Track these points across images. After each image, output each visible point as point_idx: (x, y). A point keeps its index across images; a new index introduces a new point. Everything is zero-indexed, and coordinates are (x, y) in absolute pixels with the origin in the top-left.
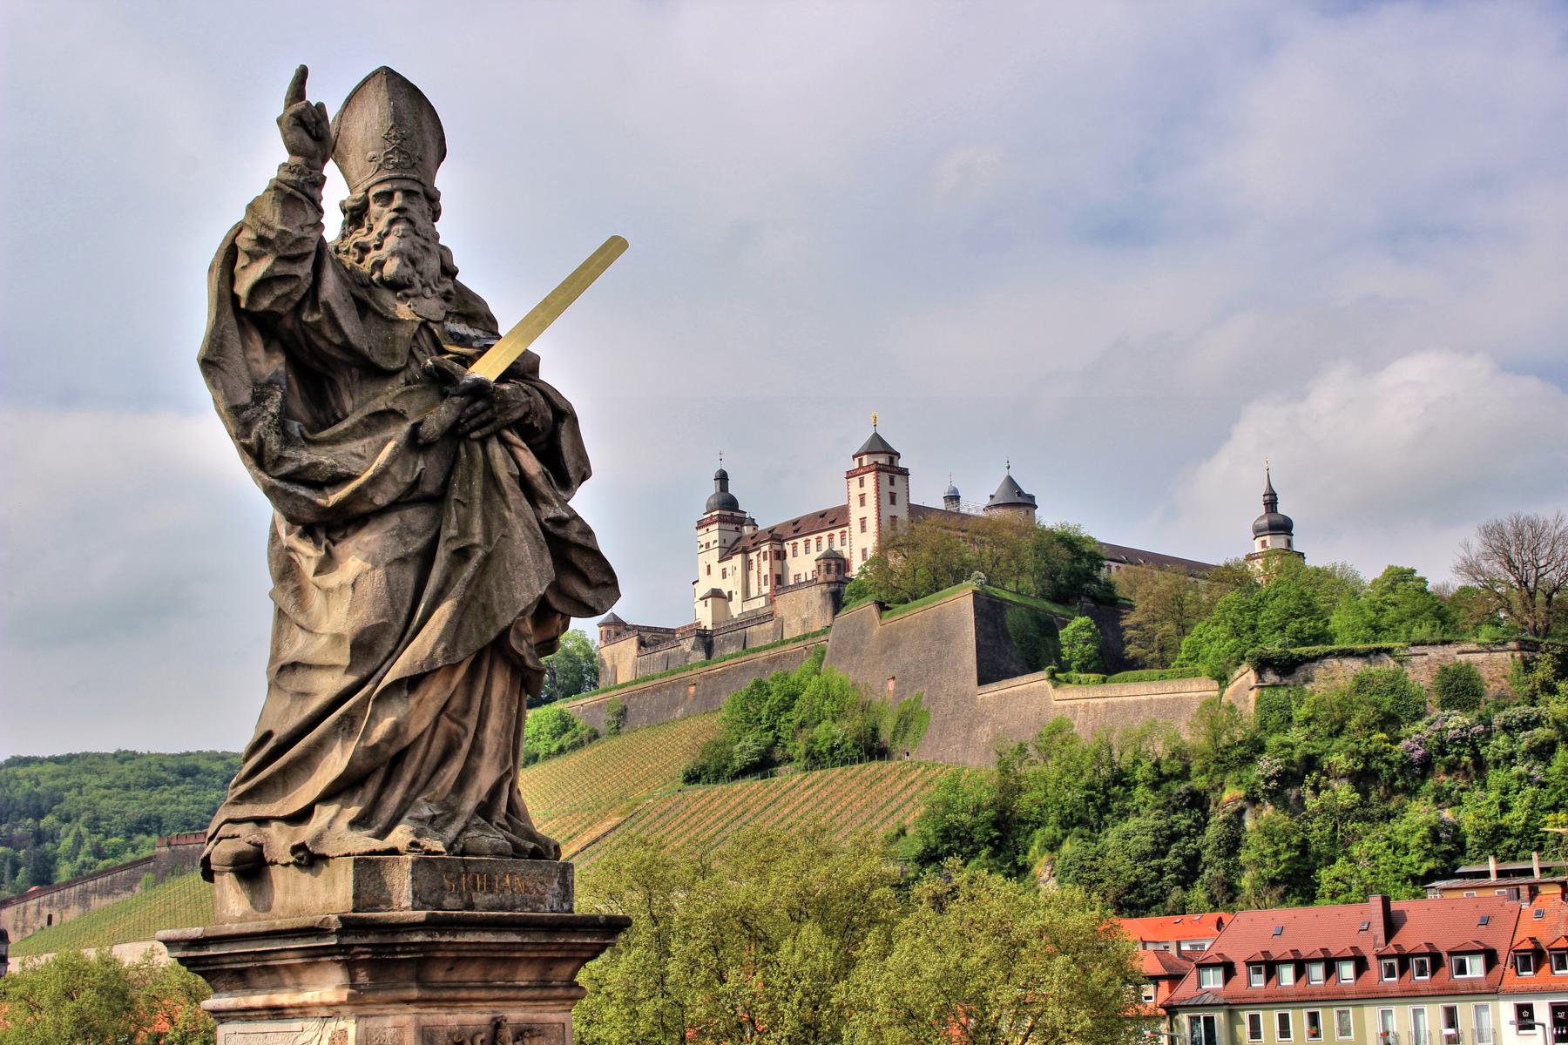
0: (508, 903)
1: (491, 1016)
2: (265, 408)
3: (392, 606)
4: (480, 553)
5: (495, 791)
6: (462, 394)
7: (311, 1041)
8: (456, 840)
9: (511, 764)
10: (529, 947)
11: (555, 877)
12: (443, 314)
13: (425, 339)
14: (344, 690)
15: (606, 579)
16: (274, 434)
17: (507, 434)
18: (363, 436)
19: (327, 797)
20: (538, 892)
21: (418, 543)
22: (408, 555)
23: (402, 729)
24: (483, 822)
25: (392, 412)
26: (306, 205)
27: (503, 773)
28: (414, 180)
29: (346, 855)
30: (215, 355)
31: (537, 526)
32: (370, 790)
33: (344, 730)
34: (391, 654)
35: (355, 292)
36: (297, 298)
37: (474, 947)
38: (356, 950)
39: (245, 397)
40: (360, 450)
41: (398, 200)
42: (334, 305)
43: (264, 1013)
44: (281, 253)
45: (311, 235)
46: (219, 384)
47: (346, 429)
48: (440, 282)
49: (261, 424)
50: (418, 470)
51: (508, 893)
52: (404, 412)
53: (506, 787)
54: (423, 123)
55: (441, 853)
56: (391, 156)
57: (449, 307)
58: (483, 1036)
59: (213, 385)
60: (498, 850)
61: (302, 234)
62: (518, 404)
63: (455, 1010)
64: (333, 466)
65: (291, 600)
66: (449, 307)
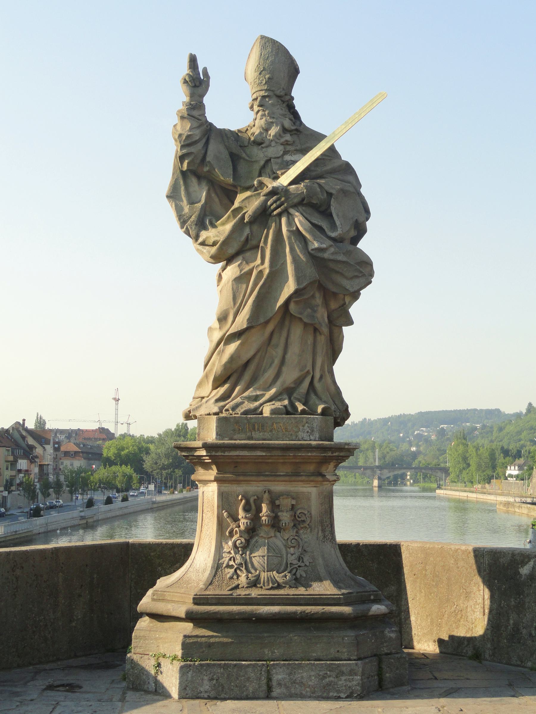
4: (267, 272)
5: (299, 382)
9: (309, 367)
12: (282, 153)
15: (356, 274)
35: (234, 151)
50: (245, 234)
58: (256, 497)
66: (289, 148)
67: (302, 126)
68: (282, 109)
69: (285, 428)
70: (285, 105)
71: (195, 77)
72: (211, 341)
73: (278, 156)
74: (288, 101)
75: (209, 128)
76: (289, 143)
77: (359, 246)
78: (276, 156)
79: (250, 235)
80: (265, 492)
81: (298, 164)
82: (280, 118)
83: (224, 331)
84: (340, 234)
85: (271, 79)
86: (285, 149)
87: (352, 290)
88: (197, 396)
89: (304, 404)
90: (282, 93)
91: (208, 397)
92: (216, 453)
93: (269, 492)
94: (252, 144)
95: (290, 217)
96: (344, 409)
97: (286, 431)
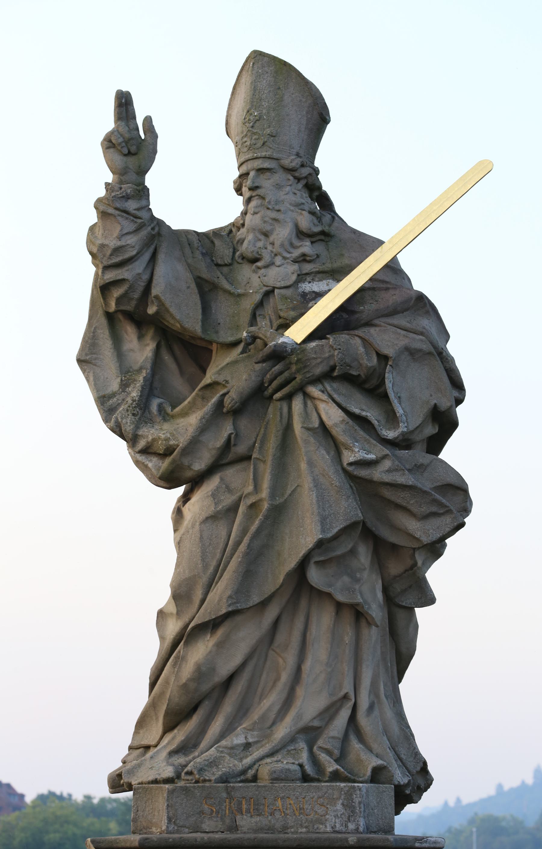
0: (278, 825)
2: (129, 393)
3: (203, 560)
4: (266, 506)
6: (263, 361)
8: (250, 767)
12: (294, 278)
14: (177, 636)
15: (434, 509)
16: (130, 416)
22: (219, 512)
26: (119, 218)
30: (86, 355)
35: (205, 275)
39: (115, 385)
44: (106, 263)
45: (129, 242)
46: (91, 379)
47: (189, 403)
50: (225, 435)
51: (277, 815)
52: (227, 382)
54: (286, 97)
56: (245, 139)
60: (275, 776)
61: (119, 243)
62: (319, 360)
64: (167, 439)
66: (308, 268)
67: (336, 224)
68: (295, 194)
69: (300, 809)
70: (300, 186)
71: (127, 136)
72: (162, 638)
73: (289, 284)
74: (306, 177)
75: (157, 229)
76: (308, 258)
77: (442, 456)
78: (283, 284)
79: (233, 436)
82: (292, 211)
83: (186, 619)
84: (403, 434)
85: (274, 136)
86: (300, 270)
87: (426, 540)
88: (136, 744)
89: (337, 761)
90: (295, 163)
91: (156, 746)
94: (240, 261)
95: (309, 403)
96: (419, 769)
97: (300, 814)
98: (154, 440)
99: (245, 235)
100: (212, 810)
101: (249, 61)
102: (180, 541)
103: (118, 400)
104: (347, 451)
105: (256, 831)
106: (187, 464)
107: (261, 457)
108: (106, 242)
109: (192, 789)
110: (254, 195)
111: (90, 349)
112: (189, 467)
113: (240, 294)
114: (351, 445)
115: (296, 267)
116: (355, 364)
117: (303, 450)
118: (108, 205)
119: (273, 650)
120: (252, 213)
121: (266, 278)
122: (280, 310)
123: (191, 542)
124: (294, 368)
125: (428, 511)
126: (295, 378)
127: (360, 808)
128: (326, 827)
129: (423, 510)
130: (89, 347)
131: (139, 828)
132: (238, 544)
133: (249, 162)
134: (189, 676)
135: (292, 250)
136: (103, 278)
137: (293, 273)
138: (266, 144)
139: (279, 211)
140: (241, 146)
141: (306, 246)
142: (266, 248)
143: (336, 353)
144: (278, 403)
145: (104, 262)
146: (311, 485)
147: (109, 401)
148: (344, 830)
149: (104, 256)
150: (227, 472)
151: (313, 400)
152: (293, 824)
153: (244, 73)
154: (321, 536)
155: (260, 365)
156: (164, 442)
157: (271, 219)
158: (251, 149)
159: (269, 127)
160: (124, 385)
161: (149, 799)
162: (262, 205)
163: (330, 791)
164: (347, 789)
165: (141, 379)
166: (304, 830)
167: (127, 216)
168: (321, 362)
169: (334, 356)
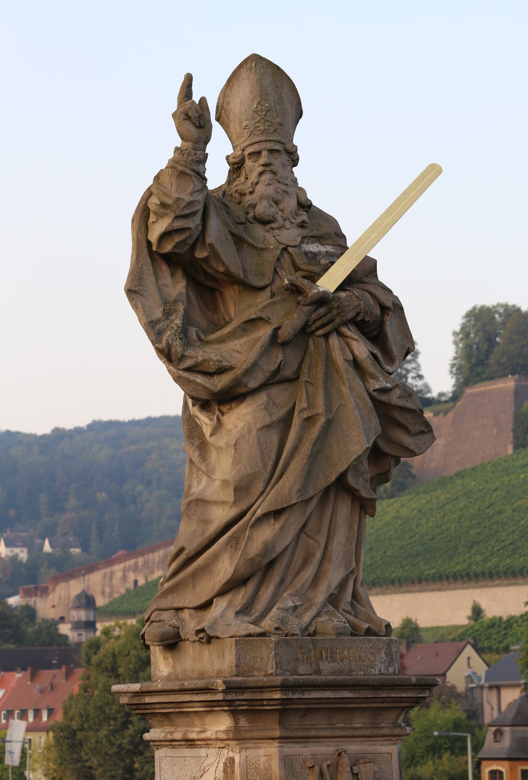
0: (346, 669)
1: (335, 748)
2: (172, 321)
3: (262, 460)
4: (322, 420)
5: (342, 585)
6: (310, 304)
7: (213, 764)
8: (310, 624)
9: (354, 565)
10: (361, 701)
11: (382, 649)
12: (299, 239)
13: (286, 261)
14: (231, 520)
15: (423, 428)
17: (345, 330)
18: (242, 336)
19: (222, 593)
20: (369, 660)
21: (279, 413)
22: (273, 422)
23: (270, 547)
24: (332, 609)
25: (260, 319)
26: (193, 178)
27: (348, 572)
28: (276, 141)
29: (231, 637)
30: (136, 286)
31: (366, 396)
32: (251, 587)
33: (231, 547)
34: (262, 493)
36: (191, 242)
37: (318, 701)
38: (237, 703)
39: (158, 314)
40: (238, 348)
41: (263, 160)
42: (217, 246)
43: (183, 743)
44: (178, 214)
45: (198, 198)
46: (140, 306)
47: (229, 332)
48: (297, 214)
49: (169, 333)
50: (278, 361)
51: (346, 661)
53: (351, 583)
54: (283, 95)
55: (297, 635)
56: (259, 124)
57: (305, 232)
58: (329, 762)
59: (135, 307)
61: (192, 199)
62: (351, 308)
63: (308, 745)
64: (219, 361)
65: (197, 453)
66: (305, 232)
76: (305, 225)
80: (340, 754)
81: (340, 262)
92: (293, 694)
93: (345, 752)
97: (359, 660)
98: (204, 361)
99: (256, 200)
100: (304, 658)
101: (249, 61)
102: (236, 443)
103: (163, 325)
104: (373, 380)
105: (332, 674)
106: (245, 382)
107: (310, 381)
108: (182, 196)
109: (291, 641)
110: (267, 169)
111: (138, 282)
112: (246, 385)
113: (262, 249)
114: (378, 376)
115: (300, 231)
116: (369, 312)
117: (345, 377)
118: (185, 166)
119: (305, 534)
120: (266, 184)
121: (279, 237)
122: (299, 264)
123: (248, 445)
124: (335, 312)
125: (419, 430)
126: (334, 320)
127: (396, 656)
128: (375, 670)
129: (416, 428)
130: (137, 280)
131: (241, 672)
132: (295, 449)
133: (261, 143)
134: (257, 552)
135: (296, 217)
136: (172, 226)
137: (298, 236)
138: (277, 130)
139: (286, 185)
140: (254, 129)
141: (305, 215)
142: (277, 214)
143: (362, 302)
144: (319, 339)
145: (176, 212)
146: (354, 405)
147: (156, 325)
148: (386, 673)
149: (178, 207)
150: (272, 390)
151: (344, 338)
152: (355, 668)
153: (243, 70)
154: (368, 446)
155: (307, 307)
156: (217, 363)
157: (282, 190)
158: (265, 132)
159: (277, 117)
160: (167, 313)
161: (250, 649)
162: (274, 179)
163: (377, 643)
164: (387, 641)
165: (181, 309)
166: (362, 673)
167: (199, 177)
168: (353, 309)
169: (360, 305)
